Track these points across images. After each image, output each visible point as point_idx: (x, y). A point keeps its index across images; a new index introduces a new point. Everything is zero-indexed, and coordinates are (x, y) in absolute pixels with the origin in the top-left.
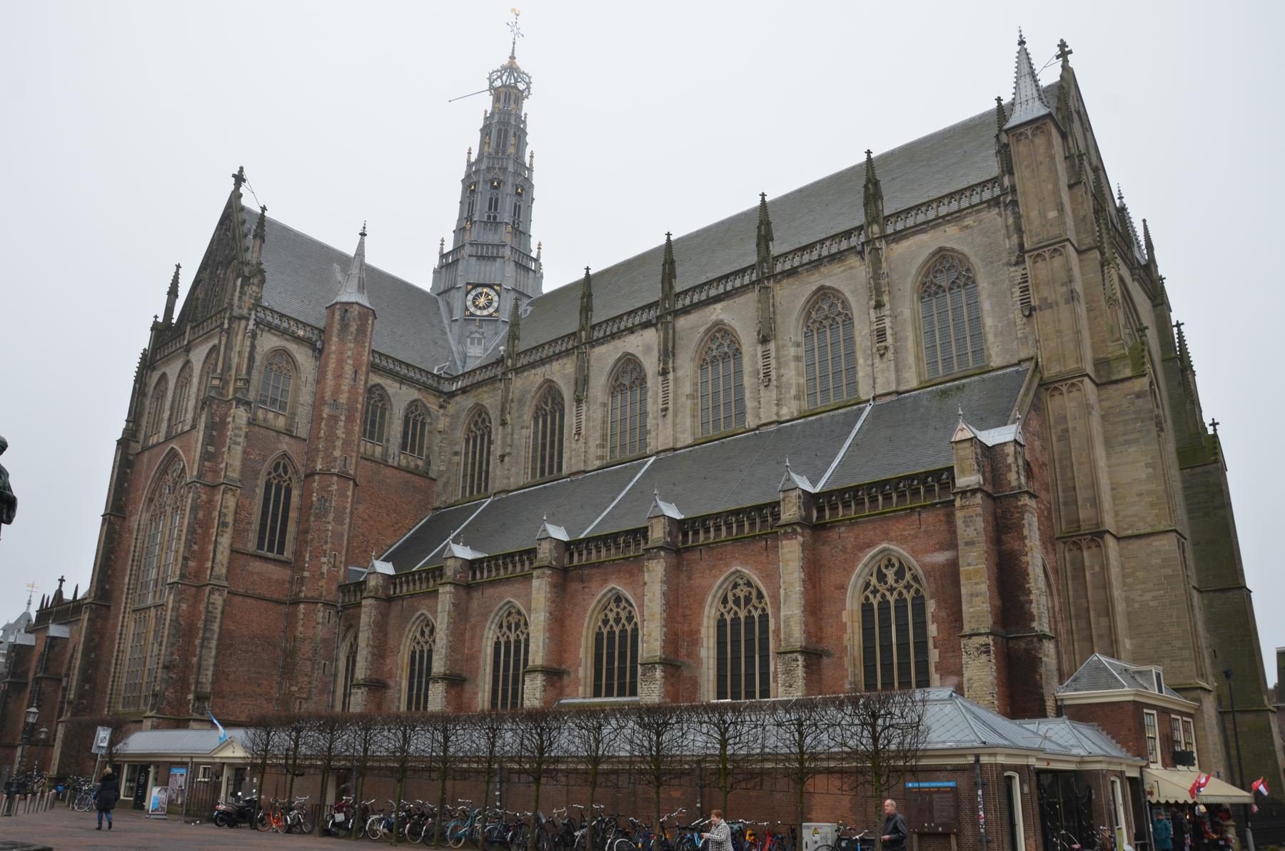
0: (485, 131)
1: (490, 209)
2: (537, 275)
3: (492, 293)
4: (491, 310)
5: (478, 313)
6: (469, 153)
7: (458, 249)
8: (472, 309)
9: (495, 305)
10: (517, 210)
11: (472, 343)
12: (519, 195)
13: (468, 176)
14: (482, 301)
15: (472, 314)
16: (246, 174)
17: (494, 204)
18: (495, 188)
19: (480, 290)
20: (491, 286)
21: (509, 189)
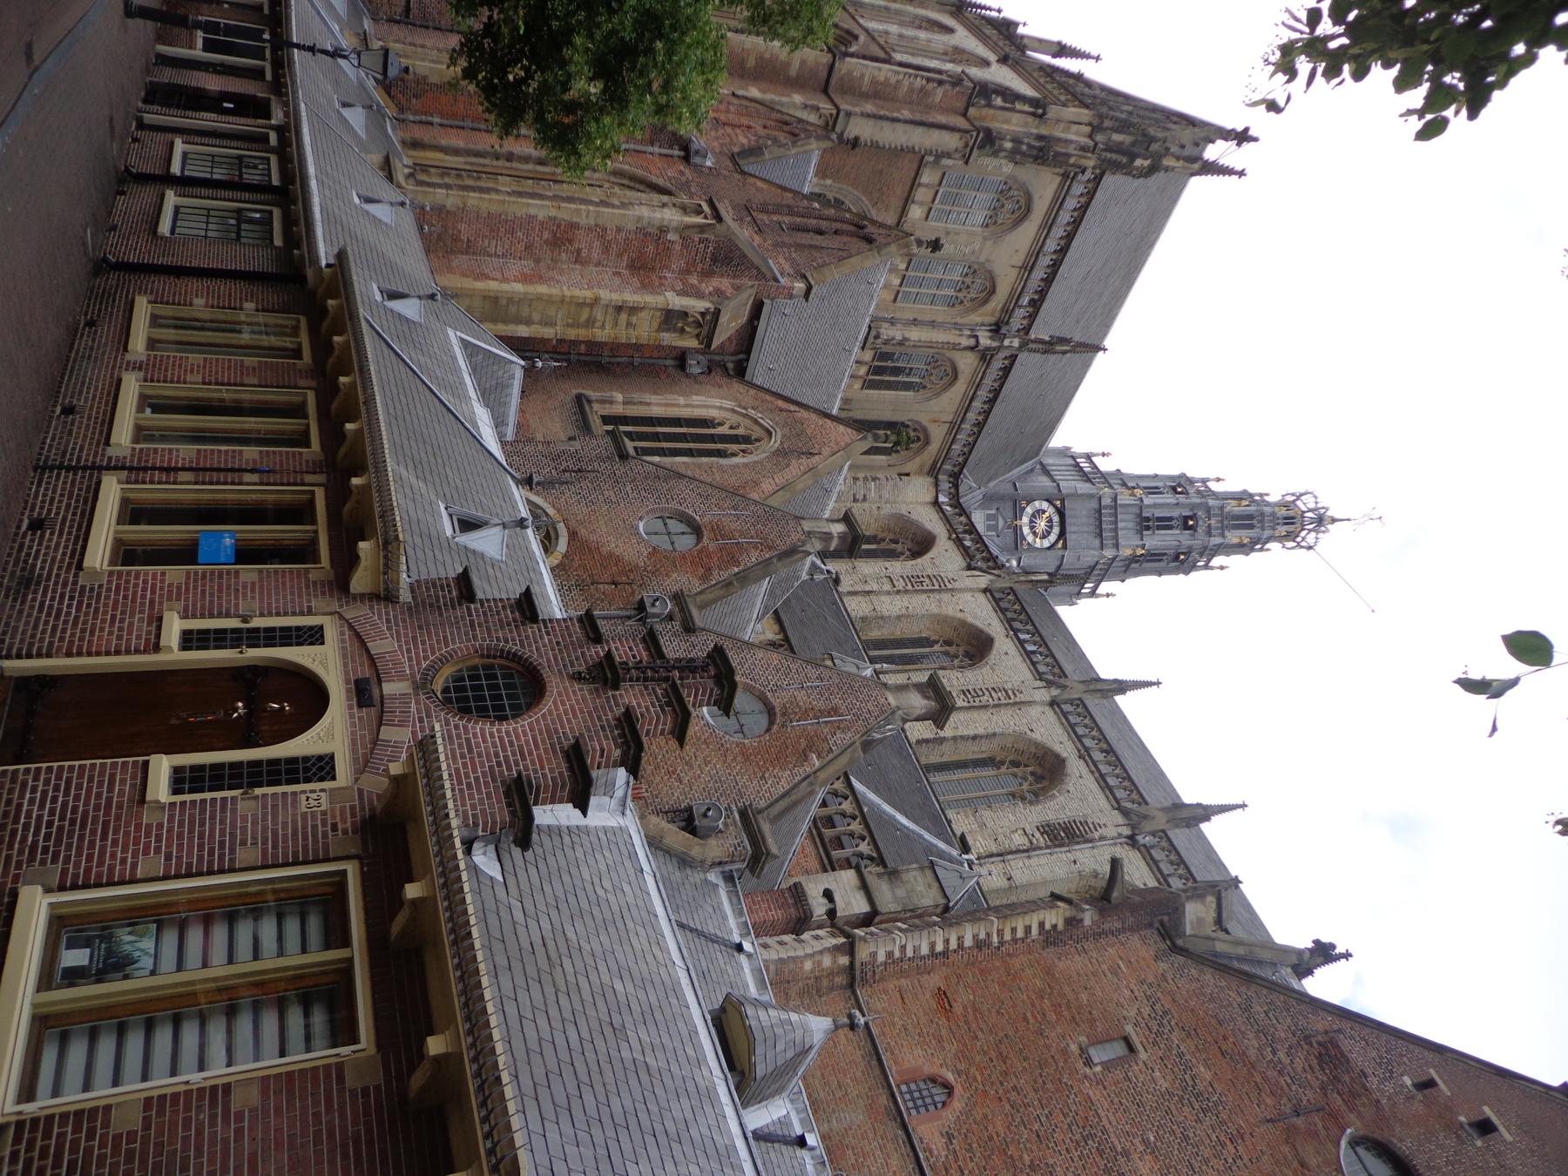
0: (1243, 496)
2: (1072, 598)
3: (1053, 537)
5: (1025, 520)
6: (1218, 480)
7: (1104, 477)
8: (1029, 510)
11: (989, 517)
12: (1176, 558)
13: (1191, 481)
14: (1042, 525)
16: (1246, 146)
17: (1165, 523)
18: (1186, 523)
19: (1056, 519)
20: (1062, 534)
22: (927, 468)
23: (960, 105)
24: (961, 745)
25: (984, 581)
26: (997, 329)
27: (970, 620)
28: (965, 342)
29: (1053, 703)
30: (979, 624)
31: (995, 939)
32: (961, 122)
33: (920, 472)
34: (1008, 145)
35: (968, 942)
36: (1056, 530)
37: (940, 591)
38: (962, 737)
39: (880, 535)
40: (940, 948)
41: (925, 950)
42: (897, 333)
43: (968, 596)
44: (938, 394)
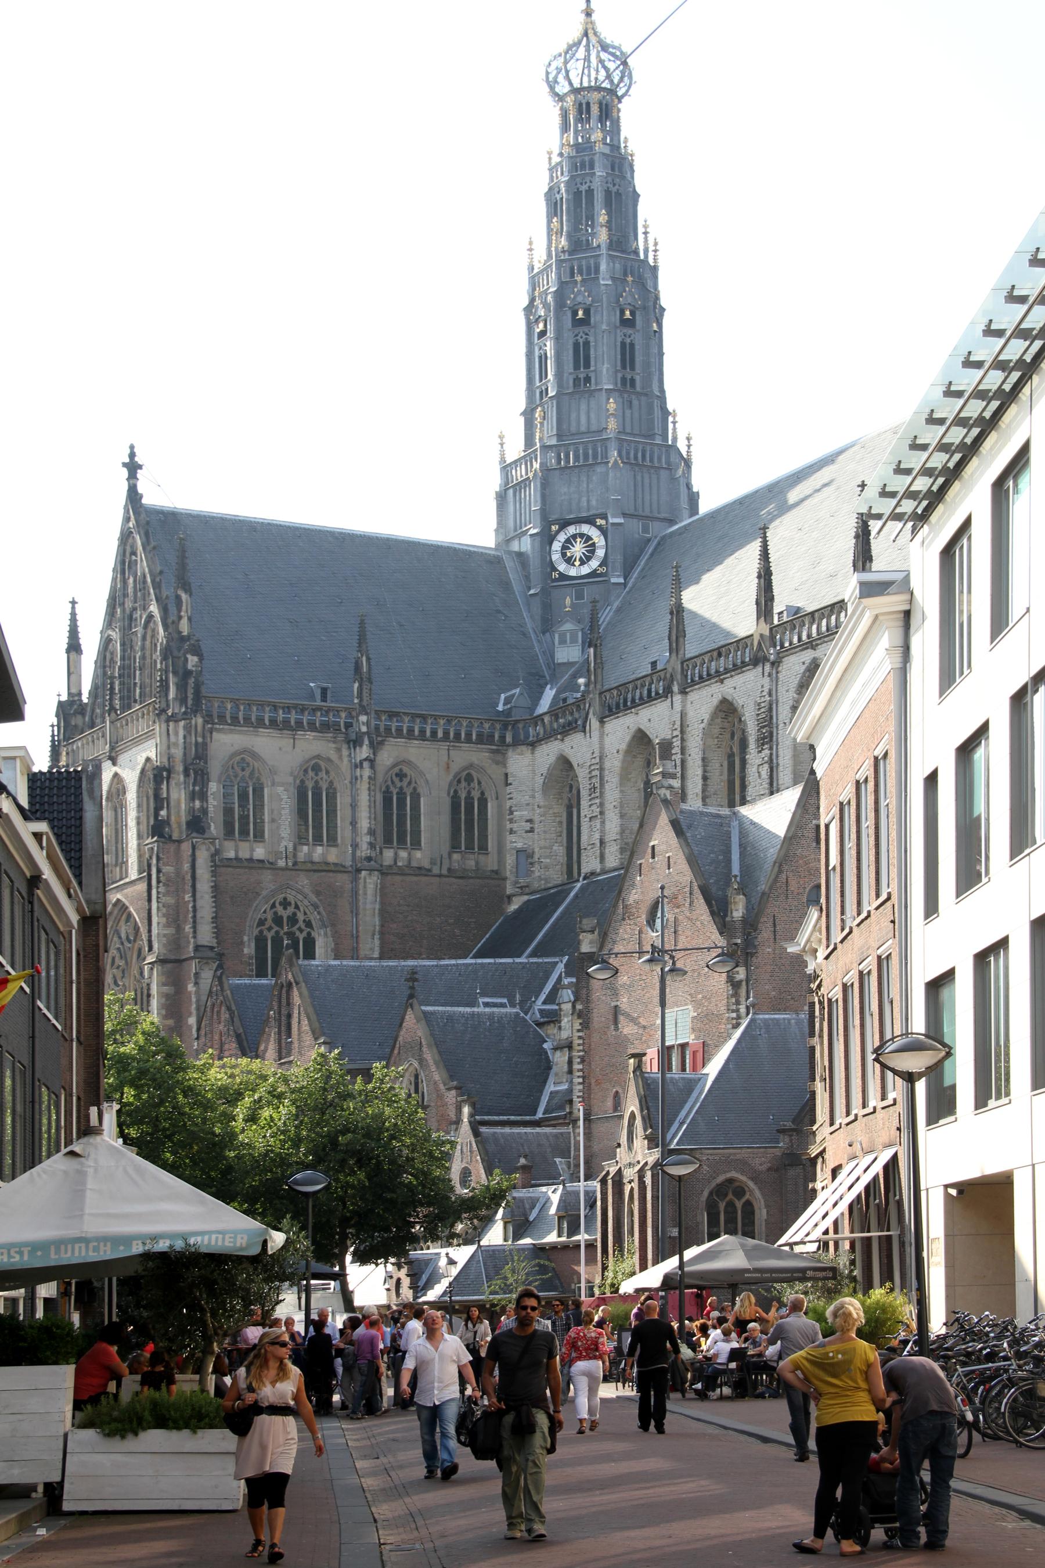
1: (577, 367)
4: (594, 564)
9: (600, 553)
10: (627, 356)
11: (563, 642)
12: (629, 323)
14: (578, 549)
15: (563, 577)
19: (572, 530)
20: (590, 521)
21: (604, 320)
22: (499, 757)
23: (172, 847)
24: (711, 789)
25: (594, 723)
26: (355, 743)
27: (623, 747)
28: (367, 772)
29: (683, 692)
30: (628, 738)
31: (581, 1053)
32: (186, 847)
33: (504, 764)
34: (197, 804)
35: (581, 1067)
36: (586, 529)
37: (601, 769)
38: (704, 791)
39: (566, 801)
40: (581, 1080)
41: (581, 1087)
42: (365, 840)
43: (607, 741)
44: (422, 774)
